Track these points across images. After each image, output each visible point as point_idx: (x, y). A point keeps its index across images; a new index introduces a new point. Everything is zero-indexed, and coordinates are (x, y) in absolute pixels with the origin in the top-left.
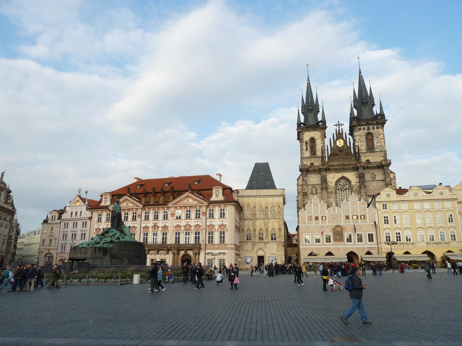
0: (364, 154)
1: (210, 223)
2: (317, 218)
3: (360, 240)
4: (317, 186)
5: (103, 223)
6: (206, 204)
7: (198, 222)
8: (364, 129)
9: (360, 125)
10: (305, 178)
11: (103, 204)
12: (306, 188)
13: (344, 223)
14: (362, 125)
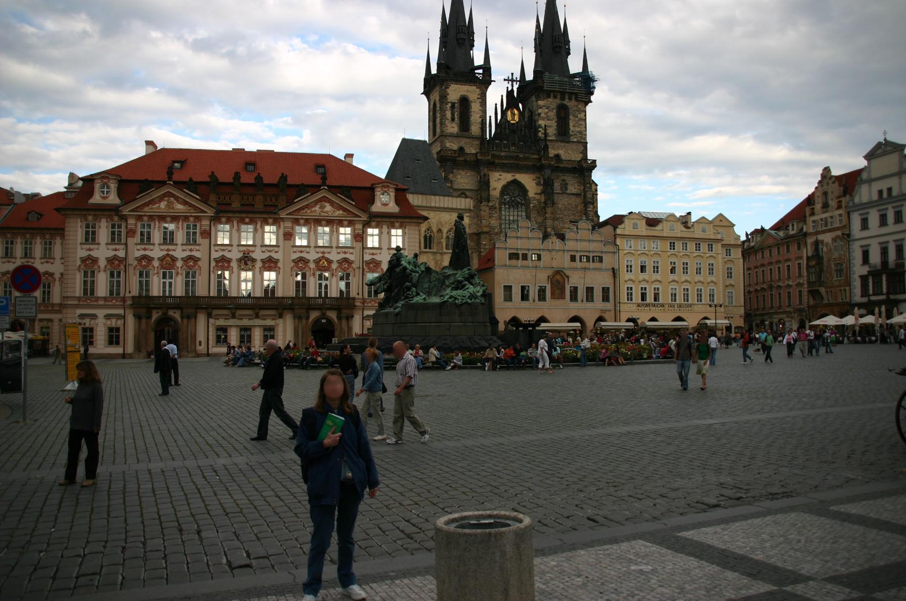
1: (372, 257)
2: (525, 257)
4: (468, 193)
5: (103, 246)
6: (364, 217)
7: (345, 253)
10: (451, 176)
11: (97, 199)
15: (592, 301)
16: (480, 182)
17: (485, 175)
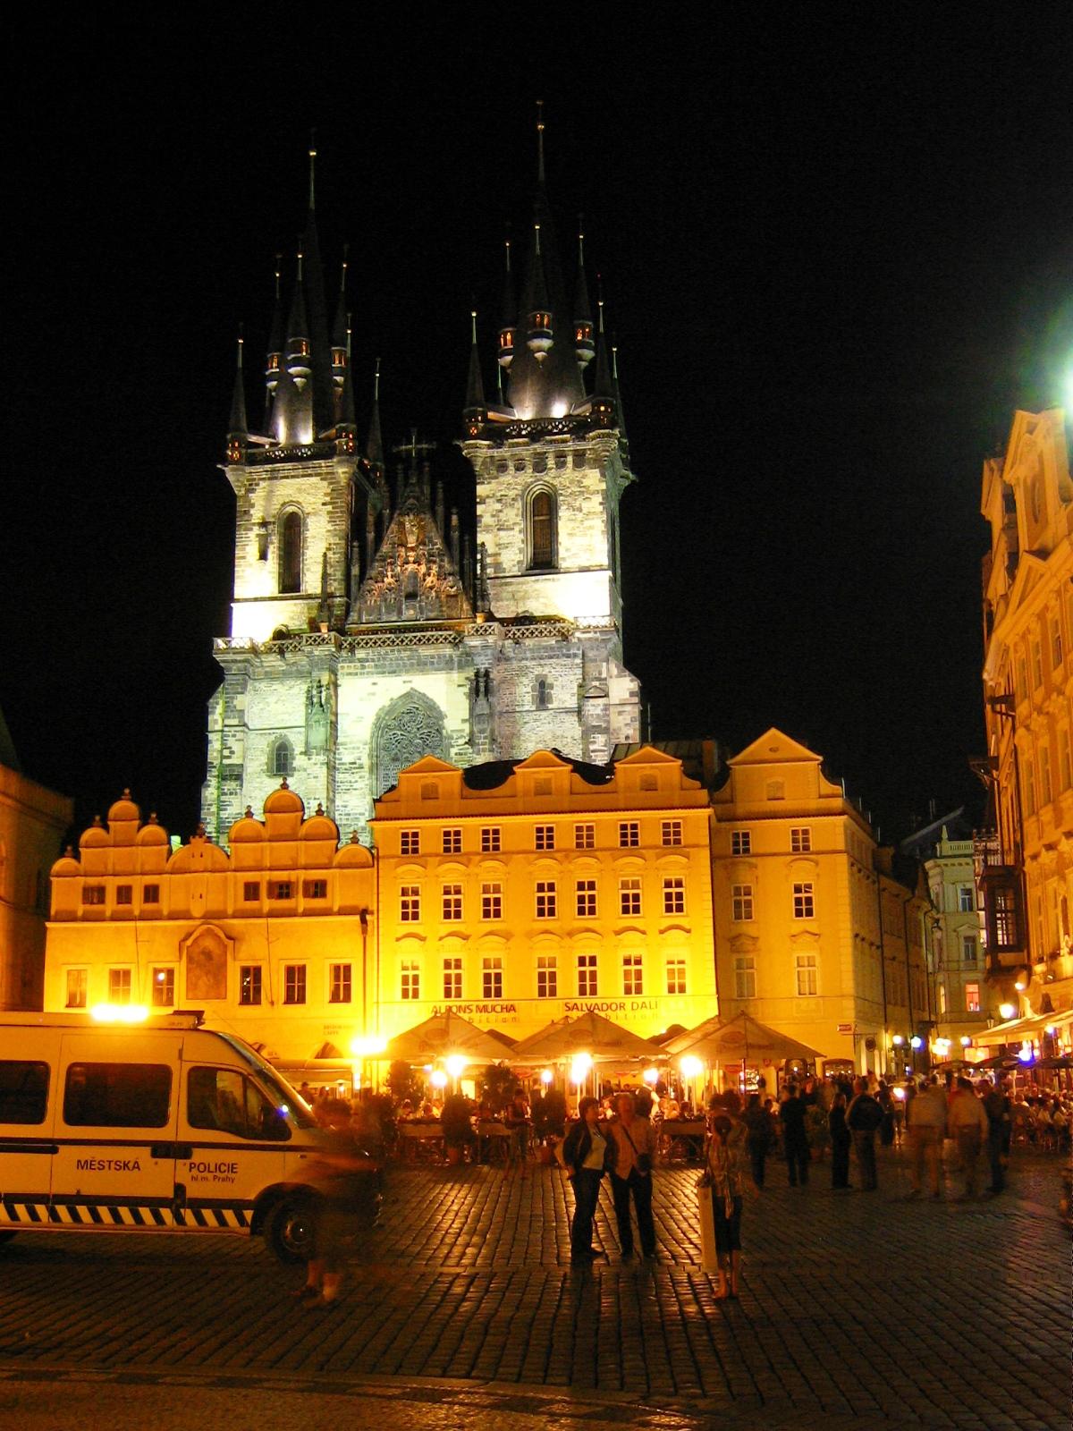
2: (124, 894)
8: (520, 468)
12: (236, 746)
15: (302, 1000)
16: (307, 705)
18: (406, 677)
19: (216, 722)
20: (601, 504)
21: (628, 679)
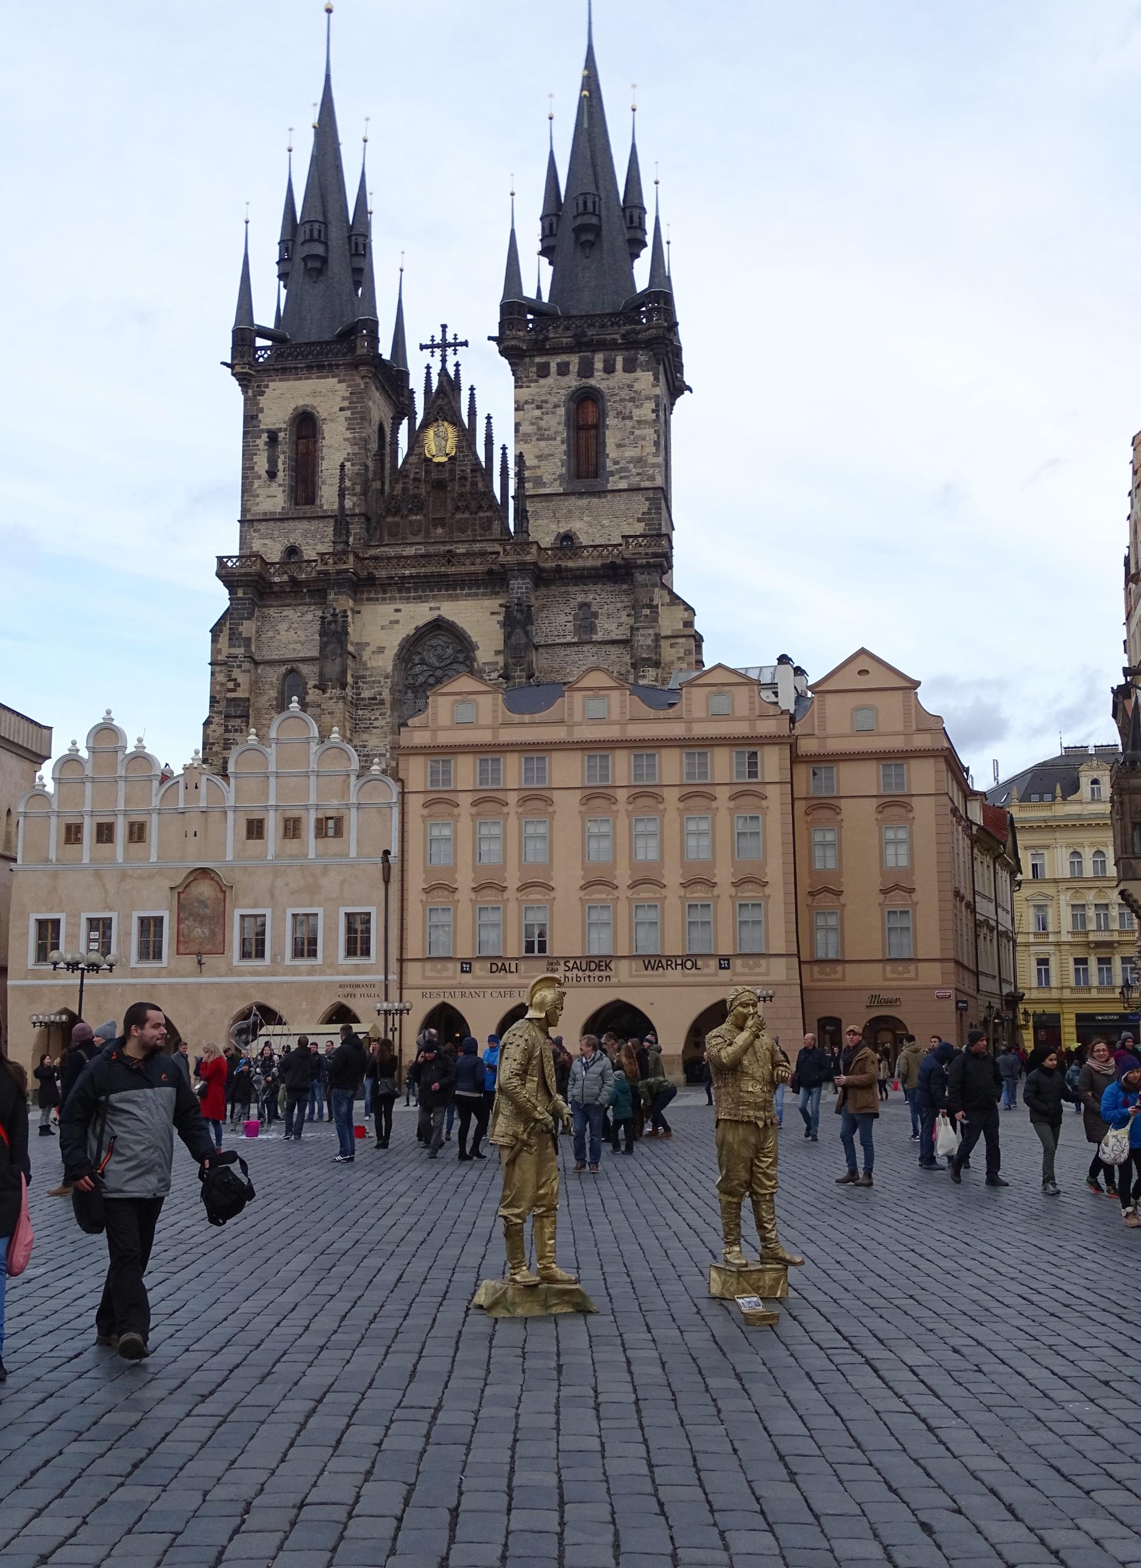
0: (552, 505)
2: (105, 833)
3: (306, 947)
4: (305, 669)
8: (563, 370)
9: (543, 352)
10: (248, 628)
12: (242, 678)
13: (237, 857)
14: (556, 351)
15: (313, 953)
17: (334, 615)
18: (432, 605)
19: (219, 651)
20: (653, 411)
21: (682, 607)
